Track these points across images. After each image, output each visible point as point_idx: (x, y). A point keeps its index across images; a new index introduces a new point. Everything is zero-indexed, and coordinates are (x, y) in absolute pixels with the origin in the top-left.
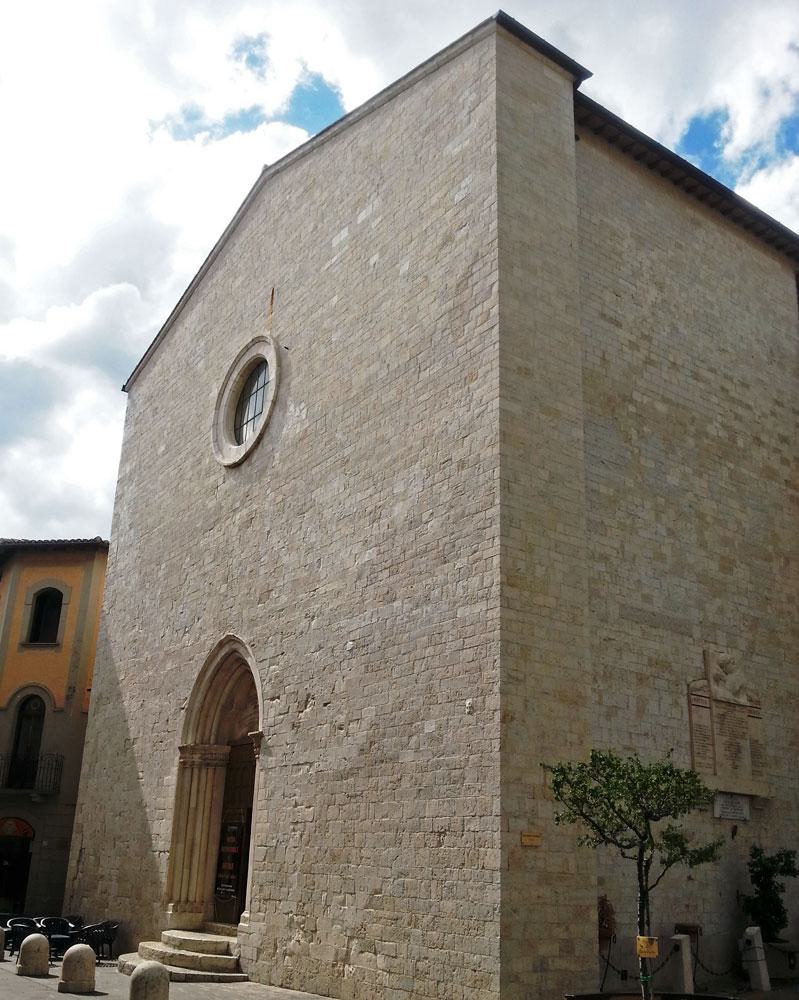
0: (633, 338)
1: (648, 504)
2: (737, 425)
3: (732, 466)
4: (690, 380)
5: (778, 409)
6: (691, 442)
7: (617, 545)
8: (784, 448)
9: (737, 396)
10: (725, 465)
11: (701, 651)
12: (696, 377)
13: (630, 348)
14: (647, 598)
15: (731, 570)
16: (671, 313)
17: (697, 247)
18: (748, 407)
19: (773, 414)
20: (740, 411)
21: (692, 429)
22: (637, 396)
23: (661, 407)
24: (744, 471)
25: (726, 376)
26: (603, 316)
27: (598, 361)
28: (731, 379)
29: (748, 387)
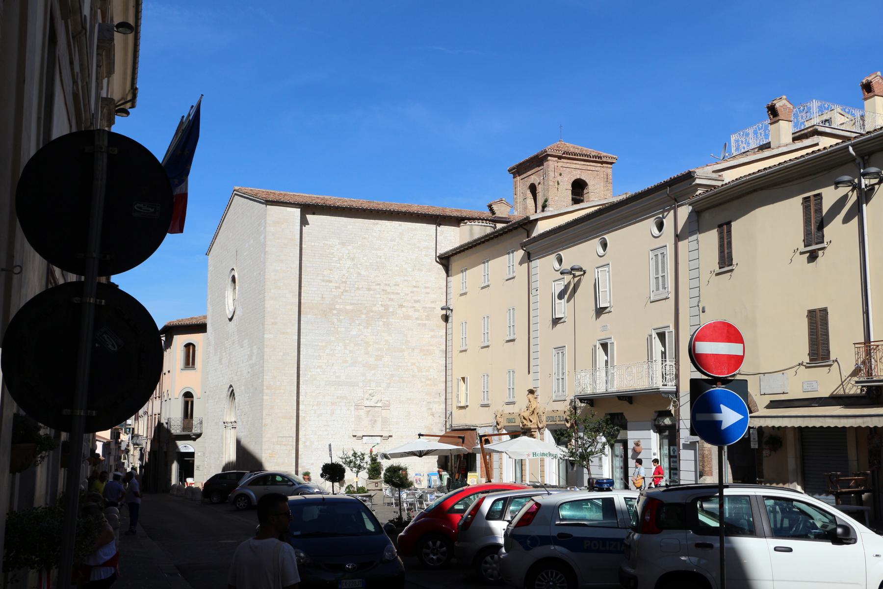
0: (337, 285)
1: (341, 344)
2: (389, 303)
3: (385, 320)
4: (367, 292)
5: (415, 289)
6: (364, 316)
7: (326, 361)
8: (417, 305)
9: (392, 291)
10: (382, 321)
11: (362, 390)
12: (369, 289)
13: (335, 289)
14: (338, 377)
15: (381, 359)
16: (357, 268)
17: (375, 234)
18: (398, 294)
19: (411, 292)
20: (392, 297)
21: (365, 311)
22: (337, 307)
23: (349, 307)
24: (391, 320)
25: (386, 285)
26: (323, 281)
27: (320, 299)
28: (389, 285)
29: (398, 285)
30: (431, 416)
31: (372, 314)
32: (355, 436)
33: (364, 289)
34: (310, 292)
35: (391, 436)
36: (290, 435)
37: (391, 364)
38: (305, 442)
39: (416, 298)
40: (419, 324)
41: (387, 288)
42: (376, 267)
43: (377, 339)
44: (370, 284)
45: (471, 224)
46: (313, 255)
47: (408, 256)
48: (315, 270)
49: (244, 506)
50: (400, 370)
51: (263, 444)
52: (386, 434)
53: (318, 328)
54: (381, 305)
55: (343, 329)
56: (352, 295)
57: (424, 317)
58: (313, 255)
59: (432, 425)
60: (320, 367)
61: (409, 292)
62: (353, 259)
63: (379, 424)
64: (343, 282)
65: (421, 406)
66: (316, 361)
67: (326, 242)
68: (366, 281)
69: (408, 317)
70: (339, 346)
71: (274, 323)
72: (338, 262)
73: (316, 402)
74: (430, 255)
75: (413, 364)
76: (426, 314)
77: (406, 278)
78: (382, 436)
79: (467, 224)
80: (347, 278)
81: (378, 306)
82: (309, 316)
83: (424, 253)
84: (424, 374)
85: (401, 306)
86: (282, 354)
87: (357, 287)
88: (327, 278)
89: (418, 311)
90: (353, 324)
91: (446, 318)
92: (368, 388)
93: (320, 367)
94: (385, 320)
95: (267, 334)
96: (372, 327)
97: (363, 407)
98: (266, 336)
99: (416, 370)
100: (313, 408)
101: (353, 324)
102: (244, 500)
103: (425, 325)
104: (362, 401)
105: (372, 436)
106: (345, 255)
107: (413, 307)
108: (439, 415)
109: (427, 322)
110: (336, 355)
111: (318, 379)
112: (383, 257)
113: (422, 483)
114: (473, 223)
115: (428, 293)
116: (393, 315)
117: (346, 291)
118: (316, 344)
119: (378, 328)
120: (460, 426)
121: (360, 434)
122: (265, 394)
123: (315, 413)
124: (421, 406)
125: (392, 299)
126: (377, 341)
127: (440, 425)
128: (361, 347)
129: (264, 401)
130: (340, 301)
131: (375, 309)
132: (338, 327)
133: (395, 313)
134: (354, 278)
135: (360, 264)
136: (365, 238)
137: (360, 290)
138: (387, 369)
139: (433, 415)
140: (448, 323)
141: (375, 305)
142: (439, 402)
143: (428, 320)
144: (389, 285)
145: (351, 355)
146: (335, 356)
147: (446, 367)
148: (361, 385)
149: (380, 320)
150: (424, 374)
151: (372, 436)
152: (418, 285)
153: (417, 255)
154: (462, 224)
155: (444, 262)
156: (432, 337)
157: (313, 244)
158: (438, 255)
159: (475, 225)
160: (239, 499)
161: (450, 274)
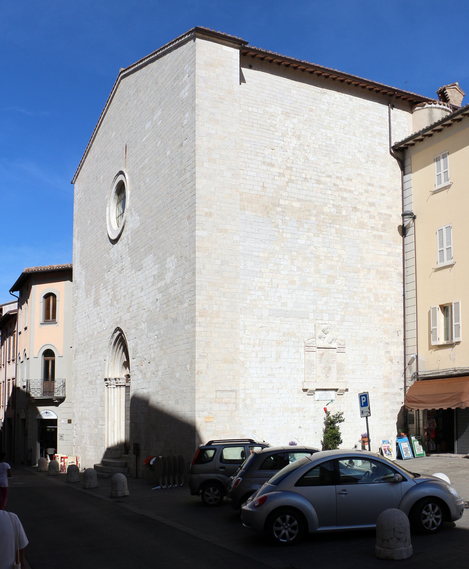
0: (281, 171)
1: (286, 257)
2: (342, 203)
3: (338, 227)
4: (316, 185)
5: (370, 188)
6: (313, 219)
7: (269, 280)
8: (372, 209)
9: (344, 187)
10: (334, 227)
11: (313, 325)
12: (318, 182)
13: (279, 176)
14: (284, 304)
15: (334, 281)
16: (304, 150)
17: (323, 107)
18: (351, 191)
19: (366, 191)
20: (345, 195)
21: (314, 212)
22: (282, 202)
23: (296, 205)
24: (345, 227)
25: (337, 178)
26: (264, 163)
27: (260, 189)
28: (340, 178)
29: (351, 180)
30: (390, 362)
31: (322, 217)
32: (305, 390)
33: (313, 181)
34: (248, 178)
35: (347, 390)
36: (232, 388)
37: (345, 288)
38: (244, 400)
39: (370, 200)
40: (375, 236)
41: (338, 182)
42: (326, 152)
43: (329, 253)
44: (320, 174)
45: (430, 106)
46: (251, 124)
47: (361, 142)
48: (253, 146)
49: (291, 535)
50: (356, 298)
51: (196, 402)
52: (341, 387)
53: (258, 231)
54: (333, 205)
55: (289, 236)
56: (299, 187)
57: (380, 226)
58: (251, 124)
59: (391, 374)
60: (261, 288)
61: (363, 191)
62: (299, 138)
63: (334, 373)
64: (288, 168)
65: (379, 349)
66: (256, 279)
67: (266, 109)
68: (316, 169)
69: (362, 225)
70: (284, 259)
71: (209, 215)
72: (281, 138)
73: (258, 341)
74: (384, 144)
75: (369, 290)
76: (382, 222)
77: (359, 172)
78: (336, 390)
79: (426, 106)
80: (293, 163)
81: (330, 206)
82: (247, 212)
83: (377, 140)
84: (381, 304)
85: (355, 209)
86: (219, 262)
87: (304, 176)
88: (268, 160)
89: (374, 217)
90: (301, 229)
91: (403, 231)
92: (320, 322)
93: (261, 288)
94: (338, 227)
95: (199, 230)
96: (323, 234)
97: (315, 349)
98: (198, 233)
99: (372, 299)
100: (254, 349)
101: (301, 229)
102: (291, 521)
103: (380, 237)
104: (314, 339)
105: (325, 390)
106: (289, 130)
107: (368, 212)
108: (398, 360)
109: (382, 234)
110: (282, 272)
111: (260, 306)
112: (333, 139)
113: (392, 453)
114: (433, 105)
115: (383, 195)
116: (346, 220)
117: (291, 181)
118: (257, 254)
119: (330, 237)
120: (439, 373)
121: (312, 387)
122: (197, 324)
123: (256, 357)
124: (379, 349)
125: (345, 198)
126: (329, 255)
127: (399, 374)
128: (310, 263)
129: (197, 334)
130: (285, 194)
131: (326, 210)
132: (283, 232)
133: (348, 218)
134: (301, 163)
135: (307, 146)
136: (311, 110)
137: (307, 181)
138: (341, 296)
139: (391, 361)
140: (405, 237)
141: (326, 204)
142: (397, 342)
143: (384, 231)
144: (340, 178)
145: (300, 273)
146: (280, 273)
147: (404, 295)
148: (311, 316)
149: (332, 225)
150: (381, 304)
151: (325, 390)
152: (372, 183)
153: (370, 142)
154: (417, 108)
155: (399, 155)
156: (389, 254)
157: (250, 109)
158: (393, 145)
159: (436, 108)
160: (279, 520)
161: (407, 171)
